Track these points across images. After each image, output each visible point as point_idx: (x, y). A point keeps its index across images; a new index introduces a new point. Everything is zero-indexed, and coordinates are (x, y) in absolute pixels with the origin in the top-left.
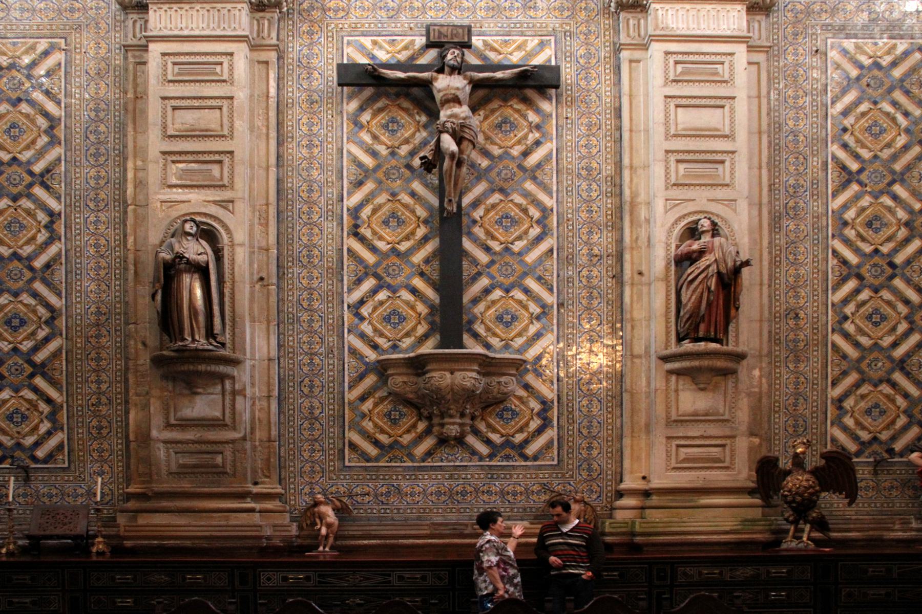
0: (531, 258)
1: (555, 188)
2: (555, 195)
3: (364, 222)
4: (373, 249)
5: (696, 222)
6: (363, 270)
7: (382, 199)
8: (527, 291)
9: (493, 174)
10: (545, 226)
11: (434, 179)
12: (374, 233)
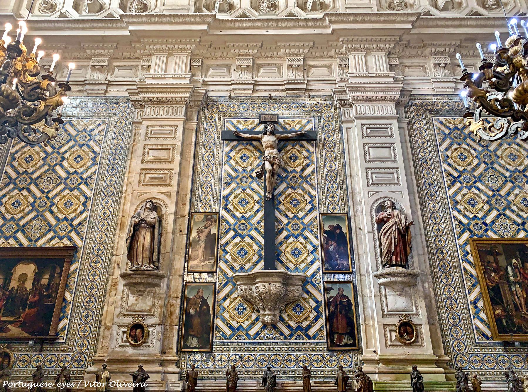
0: (307, 220)
1: (316, 186)
2: (316, 189)
4: (234, 216)
5: (384, 202)
6: (229, 227)
7: (239, 191)
8: (305, 238)
9: (288, 180)
10: (313, 205)
11: (262, 181)
12: (235, 208)
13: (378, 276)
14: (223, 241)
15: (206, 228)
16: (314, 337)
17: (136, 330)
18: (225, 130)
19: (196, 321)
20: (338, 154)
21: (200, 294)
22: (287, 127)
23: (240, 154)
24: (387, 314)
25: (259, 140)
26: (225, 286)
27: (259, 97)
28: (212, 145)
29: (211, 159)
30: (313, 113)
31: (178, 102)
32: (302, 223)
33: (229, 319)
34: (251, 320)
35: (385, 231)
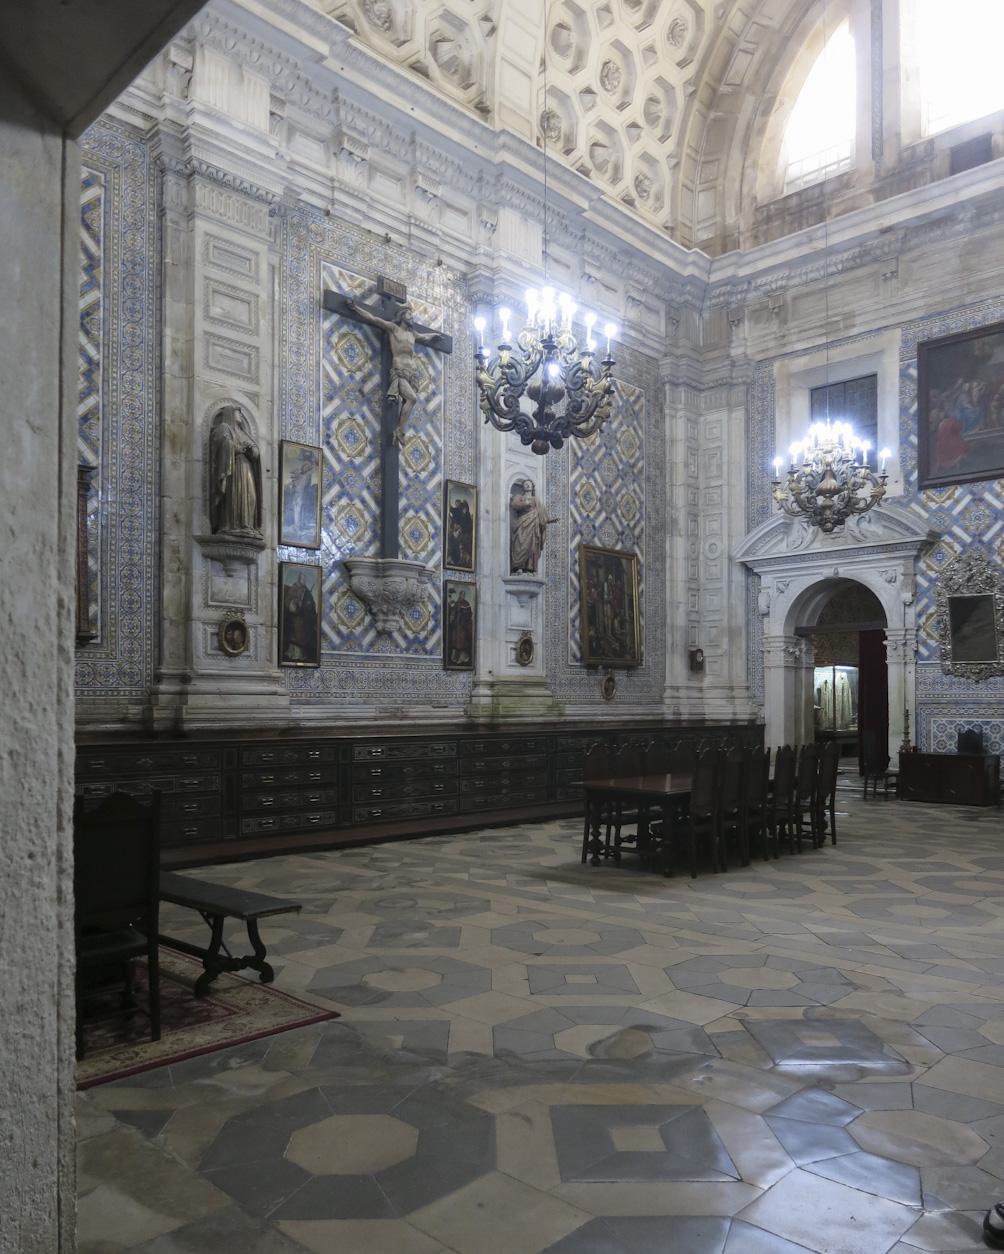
0: (431, 486)
14: (327, 499)
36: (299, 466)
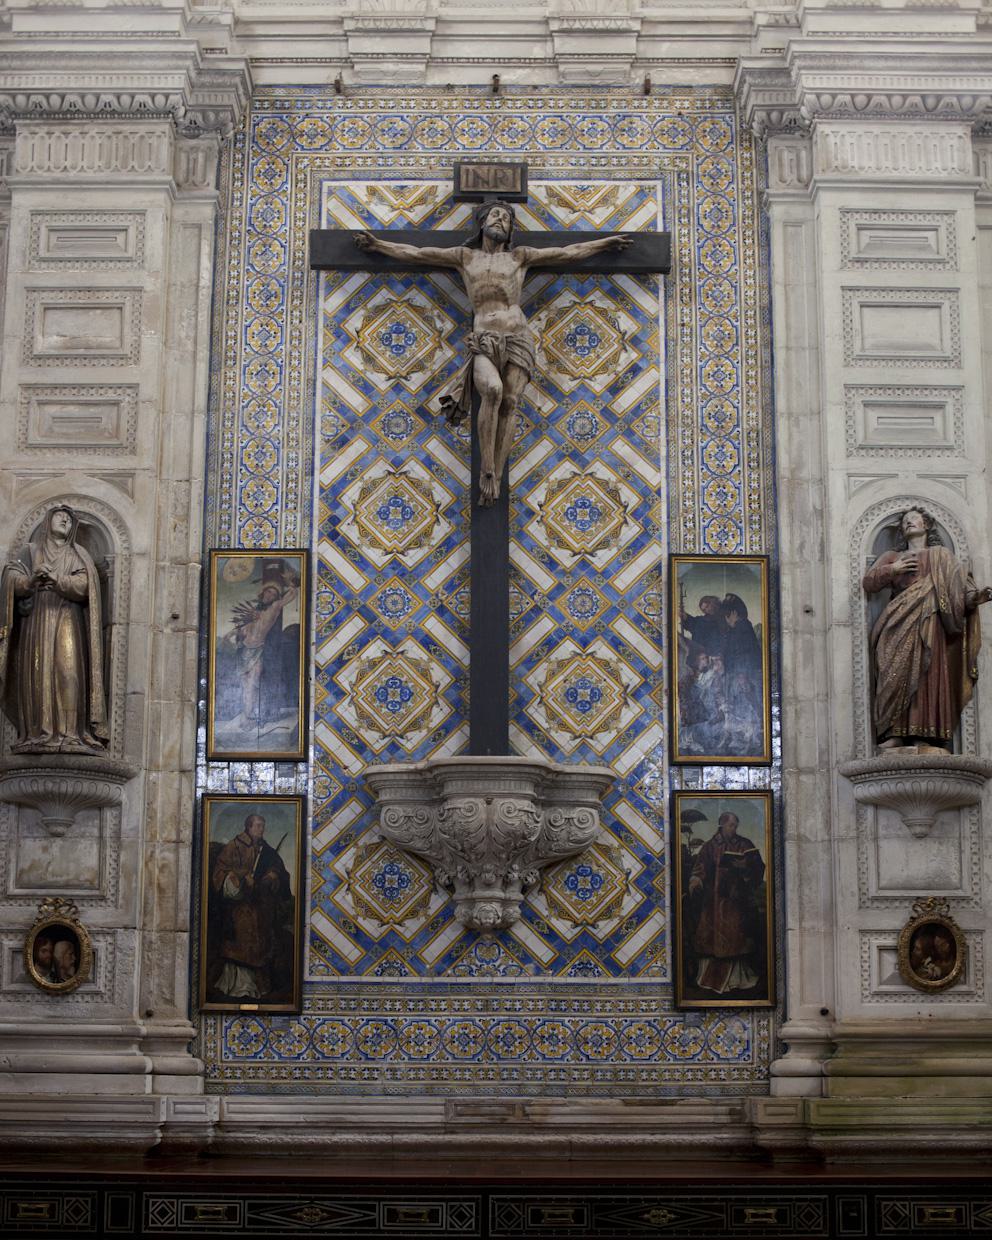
0: (624, 580)
1: (663, 453)
3: (347, 513)
4: (362, 563)
5: (901, 516)
6: (344, 603)
7: (377, 470)
8: (617, 643)
9: (562, 425)
10: (647, 523)
11: (463, 434)
12: (364, 532)
13: (854, 777)
15: (263, 606)
16: (633, 969)
17: (54, 945)
18: (324, 227)
19: (245, 921)
20: (749, 327)
21: (254, 831)
22: (561, 214)
23: (381, 325)
24: (876, 899)
25: (453, 269)
26: (337, 805)
27: (450, 87)
28: (274, 287)
29: (272, 343)
30: (659, 155)
31: (141, 113)
32: (609, 589)
33: (352, 913)
34: (427, 916)
35: (891, 623)
36: (252, 595)
